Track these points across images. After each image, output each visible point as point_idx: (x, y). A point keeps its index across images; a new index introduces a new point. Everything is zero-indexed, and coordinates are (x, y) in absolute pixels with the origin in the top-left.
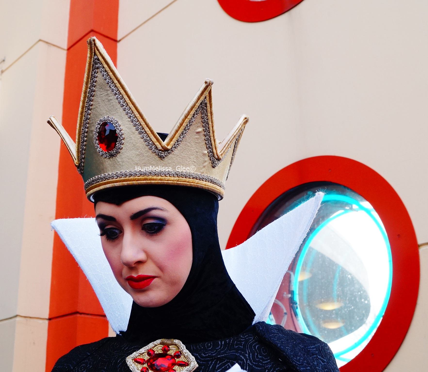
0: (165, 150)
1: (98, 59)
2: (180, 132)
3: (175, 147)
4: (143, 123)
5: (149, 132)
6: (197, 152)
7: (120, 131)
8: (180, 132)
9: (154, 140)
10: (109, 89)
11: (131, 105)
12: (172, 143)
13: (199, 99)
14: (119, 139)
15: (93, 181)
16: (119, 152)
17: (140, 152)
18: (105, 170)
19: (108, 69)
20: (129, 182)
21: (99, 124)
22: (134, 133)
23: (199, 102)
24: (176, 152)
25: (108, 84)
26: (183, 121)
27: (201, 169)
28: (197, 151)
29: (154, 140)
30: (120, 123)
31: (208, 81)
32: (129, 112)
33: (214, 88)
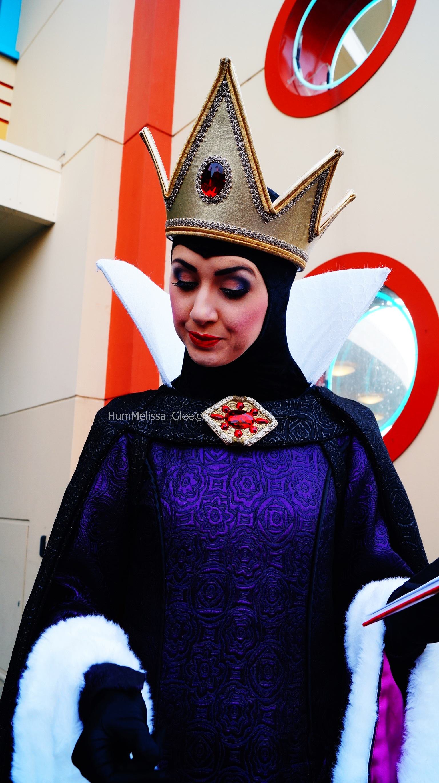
0: (272, 214)
1: (227, 86)
2: (291, 198)
3: (282, 213)
4: (257, 177)
5: (260, 189)
6: (300, 223)
7: (230, 177)
8: (291, 198)
9: (263, 199)
10: (230, 125)
11: (249, 153)
12: (280, 208)
13: (323, 166)
14: (225, 186)
15: (182, 222)
16: (222, 201)
17: (244, 208)
18: (200, 215)
19: (234, 101)
20: (223, 237)
21: (207, 162)
22: (244, 185)
23: (322, 170)
24: (281, 218)
25: (231, 118)
26: (299, 186)
27: (298, 241)
28: (300, 220)
29: (263, 199)
30: (231, 168)
31: (339, 150)
32: (246, 159)
33: (341, 160)
